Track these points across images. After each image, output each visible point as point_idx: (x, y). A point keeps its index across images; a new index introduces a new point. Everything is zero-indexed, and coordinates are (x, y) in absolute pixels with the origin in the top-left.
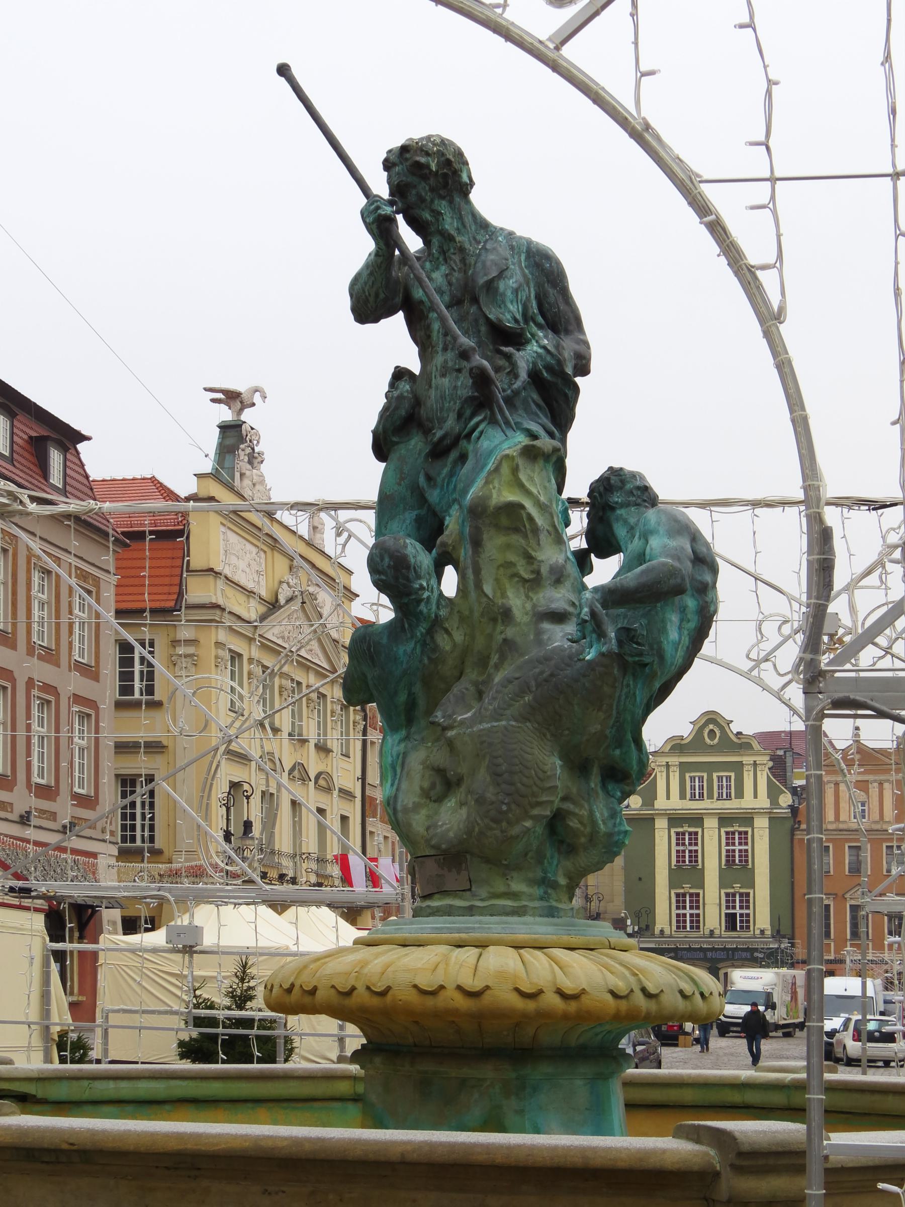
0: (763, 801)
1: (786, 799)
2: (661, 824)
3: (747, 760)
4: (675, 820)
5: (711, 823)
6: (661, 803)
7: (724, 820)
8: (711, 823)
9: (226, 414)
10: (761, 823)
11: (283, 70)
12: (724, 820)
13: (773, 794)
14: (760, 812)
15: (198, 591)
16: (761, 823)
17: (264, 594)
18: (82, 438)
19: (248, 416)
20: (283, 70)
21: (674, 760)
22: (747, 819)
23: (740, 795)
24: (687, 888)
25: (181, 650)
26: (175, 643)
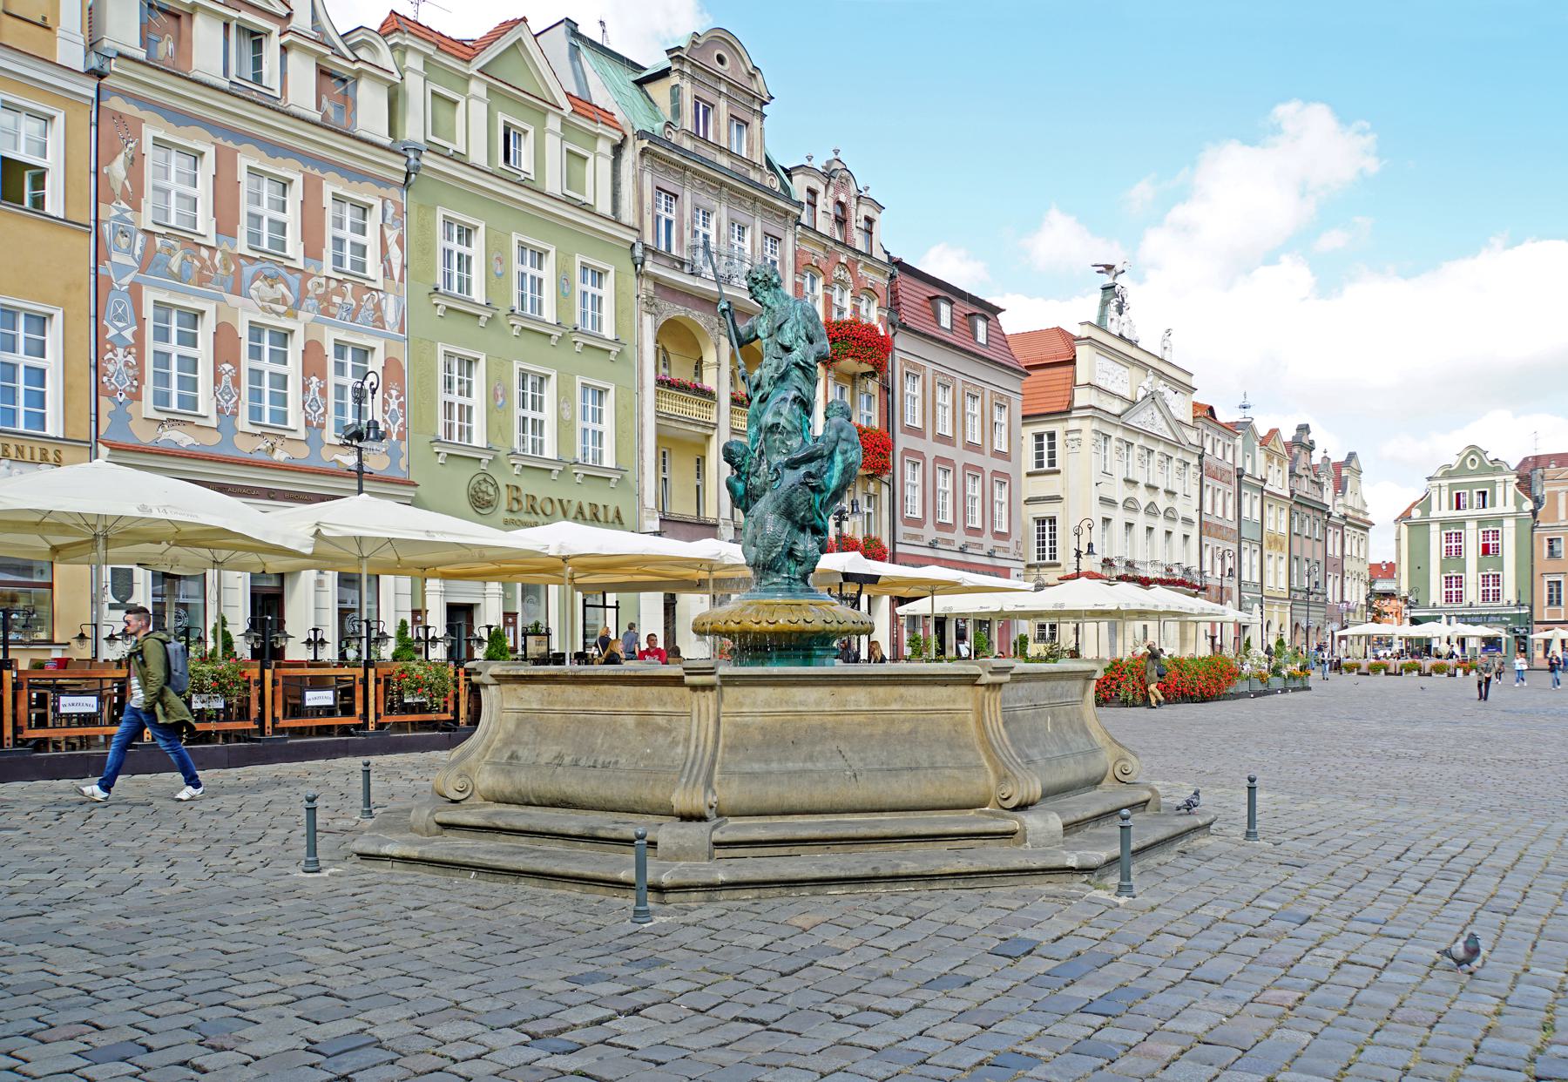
0: (1511, 508)
1: (1528, 505)
2: (1435, 528)
3: (1497, 478)
4: (1444, 524)
5: (1471, 525)
6: (1434, 513)
7: (1481, 522)
8: (1471, 525)
9: (1107, 280)
10: (1509, 524)
12: (1481, 522)
13: (1518, 502)
14: (1508, 516)
15: (1082, 397)
16: (1509, 524)
17: (1128, 396)
18: (997, 310)
19: (1121, 280)
21: (1445, 482)
22: (1499, 520)
23: (1493, 504)
24: (1491, 571)
25: (1071, 436)
26: (1067, 433)
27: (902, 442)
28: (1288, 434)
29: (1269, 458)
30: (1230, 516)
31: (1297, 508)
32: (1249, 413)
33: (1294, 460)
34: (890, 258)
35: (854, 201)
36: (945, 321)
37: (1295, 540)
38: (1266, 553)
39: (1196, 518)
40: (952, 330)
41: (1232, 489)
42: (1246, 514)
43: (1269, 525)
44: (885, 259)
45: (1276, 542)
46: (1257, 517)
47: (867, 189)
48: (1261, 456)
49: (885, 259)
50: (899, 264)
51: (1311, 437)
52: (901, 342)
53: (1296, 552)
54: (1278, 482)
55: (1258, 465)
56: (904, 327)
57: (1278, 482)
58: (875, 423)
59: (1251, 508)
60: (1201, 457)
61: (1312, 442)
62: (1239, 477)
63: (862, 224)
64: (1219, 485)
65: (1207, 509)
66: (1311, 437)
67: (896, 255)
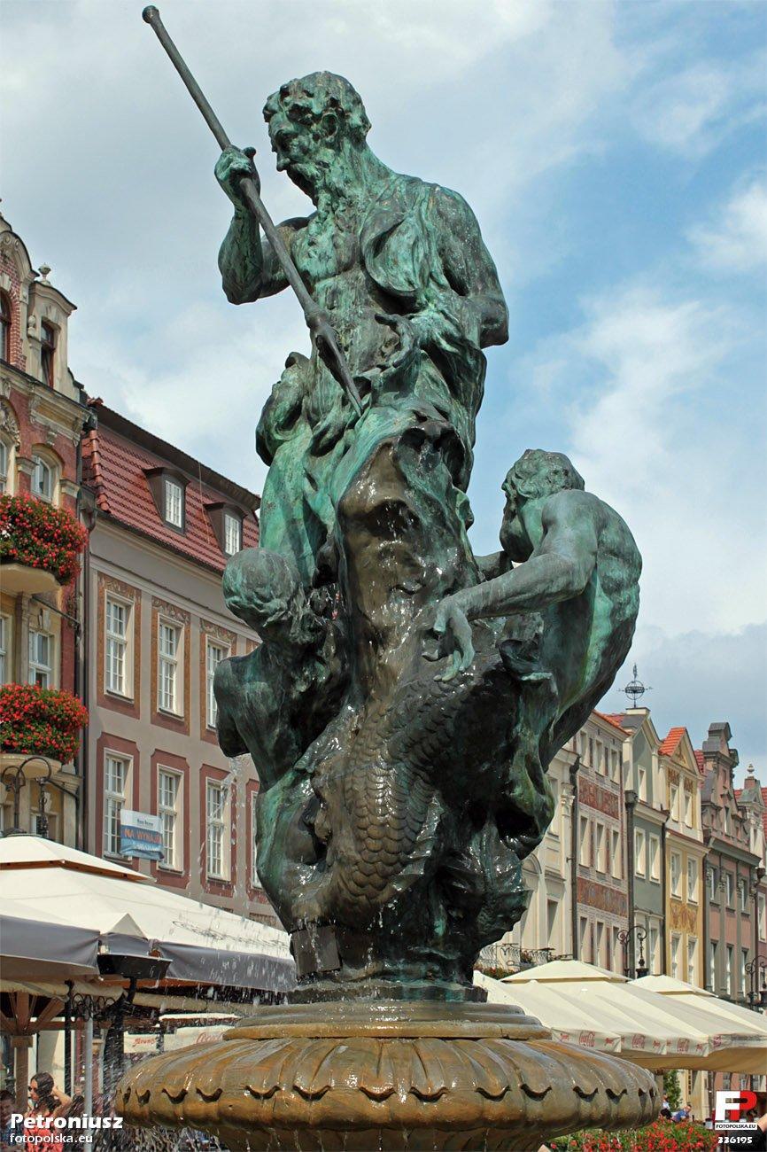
11: (150, 16)
20: (150, 16)
27: (103, 720)
28: (699, 741)
29: (672, 778)
30: (616, 872)
31: (714, 860)
32: (642, 700)
33: (707, 788)
34: (84, 396)
35: (24, 292)
36: (174, 514)
37: (713, 917)
38: (670, 933)
39: (565, 872)
40: (184, 530)
41: (617, 826)
42: (639, 868)
43: (675, 890)
44: (74, 396)
45: (684, 916)
46: (655, 873)
47: (46, 271)
48: (659, 776)
49: (75, 397)
50: (97, 405)
51: (732, 744)
52: (102, 542)
53: (713, 934)
54: (686, 818)
55: (654, 788)
56: (107, 516)
57: (686, 818)
58: (53, 684)
59: (647, 864)
60: (574, 769)
61: (734, 754)
62: (630, 806)
63: (39, 333)
64: (600, 818)
65: (583, 859)
66: (732, 744)
67: (92, 394)
